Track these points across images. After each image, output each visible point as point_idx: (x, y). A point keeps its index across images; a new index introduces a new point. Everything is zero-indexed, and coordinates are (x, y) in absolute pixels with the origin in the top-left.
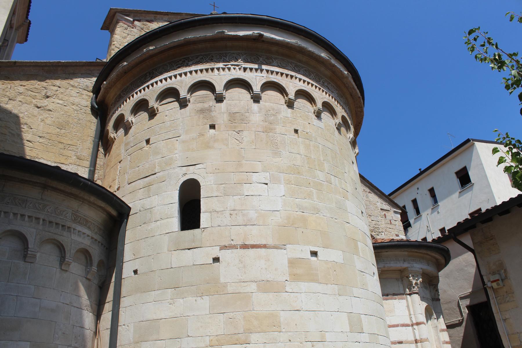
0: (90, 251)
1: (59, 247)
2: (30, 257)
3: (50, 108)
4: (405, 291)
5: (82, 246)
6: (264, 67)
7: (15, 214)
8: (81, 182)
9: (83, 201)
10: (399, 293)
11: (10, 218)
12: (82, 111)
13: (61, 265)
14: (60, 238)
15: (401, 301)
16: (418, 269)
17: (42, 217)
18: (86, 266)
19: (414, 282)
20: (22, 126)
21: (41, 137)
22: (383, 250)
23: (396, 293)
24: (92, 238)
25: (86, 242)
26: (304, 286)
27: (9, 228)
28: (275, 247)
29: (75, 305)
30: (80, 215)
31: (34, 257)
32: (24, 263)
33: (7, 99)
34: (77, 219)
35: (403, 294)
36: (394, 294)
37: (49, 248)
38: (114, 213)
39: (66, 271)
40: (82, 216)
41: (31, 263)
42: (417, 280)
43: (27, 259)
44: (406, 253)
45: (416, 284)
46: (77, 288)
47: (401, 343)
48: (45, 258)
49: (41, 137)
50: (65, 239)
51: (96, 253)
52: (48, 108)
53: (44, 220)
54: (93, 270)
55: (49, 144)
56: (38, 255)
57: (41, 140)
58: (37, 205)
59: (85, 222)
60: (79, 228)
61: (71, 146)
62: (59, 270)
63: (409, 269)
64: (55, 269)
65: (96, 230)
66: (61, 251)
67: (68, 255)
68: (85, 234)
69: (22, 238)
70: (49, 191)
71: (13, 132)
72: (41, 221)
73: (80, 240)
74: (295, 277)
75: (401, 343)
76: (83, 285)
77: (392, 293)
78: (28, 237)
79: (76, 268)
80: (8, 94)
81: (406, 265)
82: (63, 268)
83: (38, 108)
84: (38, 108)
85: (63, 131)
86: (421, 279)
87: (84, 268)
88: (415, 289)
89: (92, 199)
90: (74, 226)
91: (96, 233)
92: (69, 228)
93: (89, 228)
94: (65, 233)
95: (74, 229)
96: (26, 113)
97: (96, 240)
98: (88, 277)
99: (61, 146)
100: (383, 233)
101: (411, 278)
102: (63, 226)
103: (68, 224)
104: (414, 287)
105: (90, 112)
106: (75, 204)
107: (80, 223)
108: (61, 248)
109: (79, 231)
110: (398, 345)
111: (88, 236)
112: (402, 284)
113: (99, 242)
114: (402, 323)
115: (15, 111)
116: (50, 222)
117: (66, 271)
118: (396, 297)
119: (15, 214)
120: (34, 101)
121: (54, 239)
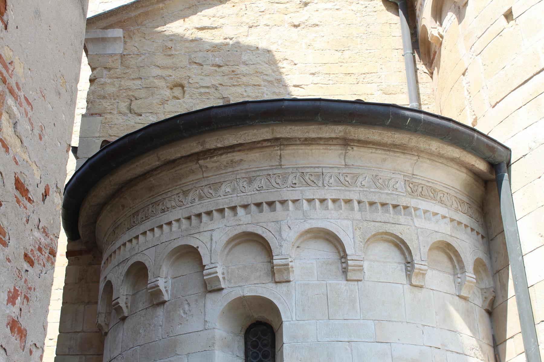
0: (455, 245)
1: (396, 245)
2: (354, 270)
3: (316, 22)
5: (439, 237)
7: (310, 201)
8: (406, 118)
9: (419, 152)
11: (305, 208)
12: (368, 10)
13: (409, 277)
14: (396, 230)
17: (355, 197)
18: (455, 275)
20: (280, 65)
21: (313, 74)
24: (452, 220)
25: (444, 230)
27: (307, 226)
30: (420, 182)
31: (360, 269)
32: (345, 282)
33: (246, 28)
34: (416, 189)
38: (481, 166)
39: (421, 287)
40: (424, 182)
41: (358, 281)
43: (350, 275)
46: (447, 317)
48: (379, 266)
49: (313, 74)
50: (405, 228)
51: (469, 247)
52: (311, 22)
53: (359, 202)
54: (468, 278)
55: (331, 82)
56: (366, 265)
57: (316, 79)
58: (342, 179)
59: (431, 193)
60: (423, 205)
61: (368, 76)
62: (407, 287)
64: (401, 286)
65: (455, 205)
66: (403, 254)
68: (437, 214)
69: (332, 239)
70: (355, 148)
71: (270, 79)
76: (457, 310)
78: (341, 236)
79: (437, 279)
80: (244, 19)
82: (414, 283)
83: (296, 26)
84: (296, 26)
85: (347, 54)
87: (451, 278)
89: (435, 145)
90: (413, 202)
91: (456, 210)
92: (406, 208)
93: (441, 202)
94: (402, 219)
95: (416, 209)
96: (280, 42)
97: (459, 223)
98: (462, 294)
99: (352, 79)
102: (395, 206)
103: (403, 201)
105: (383, 8)
106: (405, 163)
108: (401, 246)
109: (425, 212)
111: (444, 217)
113: (466, 226)
115: (263, 45)
116: (372, 204)
117: (421, 287)
119: (310, 201)
120: (286, 18)
121: (386, 233)
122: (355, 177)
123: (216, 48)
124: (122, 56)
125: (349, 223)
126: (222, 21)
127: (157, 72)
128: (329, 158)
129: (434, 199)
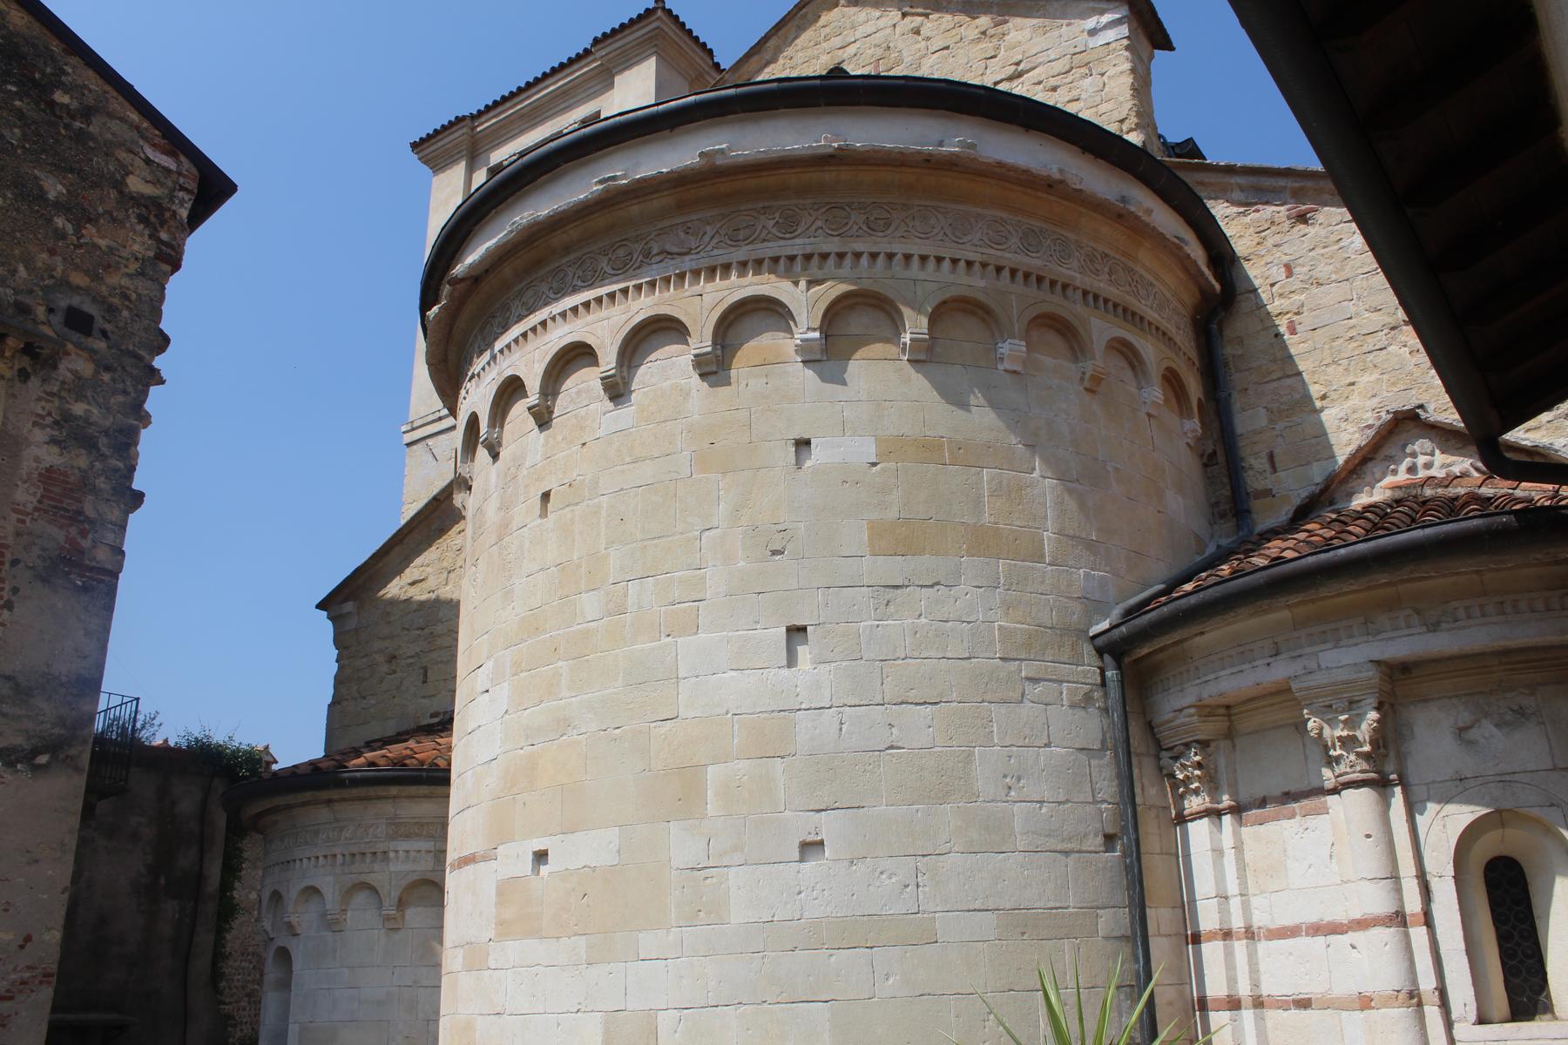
6: (498, 345)
10: (1304, 786)
14: (370, 879)
15: (1312, 821)
16: (1342, 675)
17: (337, 850)
26: (514, 949)
27: (303, 885)
28: (487, 858)
29: (425, 983)
36: (1289, 797)
37: (361, 898)
42: (1352, 724)
44: (1284, 615)
45: (1349, 742)
47: (1304, 1004)
48: (361, 914)
60: (403, 845)
63: (1294, 686)
67: (386, 903)
72: (339, 857)
73: (409, 867)
74: (505, 929)
75: (1304, 1004)
77: (1278, 793)
80: (445, 564)
86: (1373, 715)
90: (393, 845)
103: (381, 847)
106: (388, 808)
107: (407, 836)
110: (1295, 1014)
114: (1312, 918)
122: (341, 829)
123: (422, 604)
124: (356, 630)
125: (330, 878)
126: (429, 569)
127: (378, 645)
128: (323, 814)
129: (418, 835)
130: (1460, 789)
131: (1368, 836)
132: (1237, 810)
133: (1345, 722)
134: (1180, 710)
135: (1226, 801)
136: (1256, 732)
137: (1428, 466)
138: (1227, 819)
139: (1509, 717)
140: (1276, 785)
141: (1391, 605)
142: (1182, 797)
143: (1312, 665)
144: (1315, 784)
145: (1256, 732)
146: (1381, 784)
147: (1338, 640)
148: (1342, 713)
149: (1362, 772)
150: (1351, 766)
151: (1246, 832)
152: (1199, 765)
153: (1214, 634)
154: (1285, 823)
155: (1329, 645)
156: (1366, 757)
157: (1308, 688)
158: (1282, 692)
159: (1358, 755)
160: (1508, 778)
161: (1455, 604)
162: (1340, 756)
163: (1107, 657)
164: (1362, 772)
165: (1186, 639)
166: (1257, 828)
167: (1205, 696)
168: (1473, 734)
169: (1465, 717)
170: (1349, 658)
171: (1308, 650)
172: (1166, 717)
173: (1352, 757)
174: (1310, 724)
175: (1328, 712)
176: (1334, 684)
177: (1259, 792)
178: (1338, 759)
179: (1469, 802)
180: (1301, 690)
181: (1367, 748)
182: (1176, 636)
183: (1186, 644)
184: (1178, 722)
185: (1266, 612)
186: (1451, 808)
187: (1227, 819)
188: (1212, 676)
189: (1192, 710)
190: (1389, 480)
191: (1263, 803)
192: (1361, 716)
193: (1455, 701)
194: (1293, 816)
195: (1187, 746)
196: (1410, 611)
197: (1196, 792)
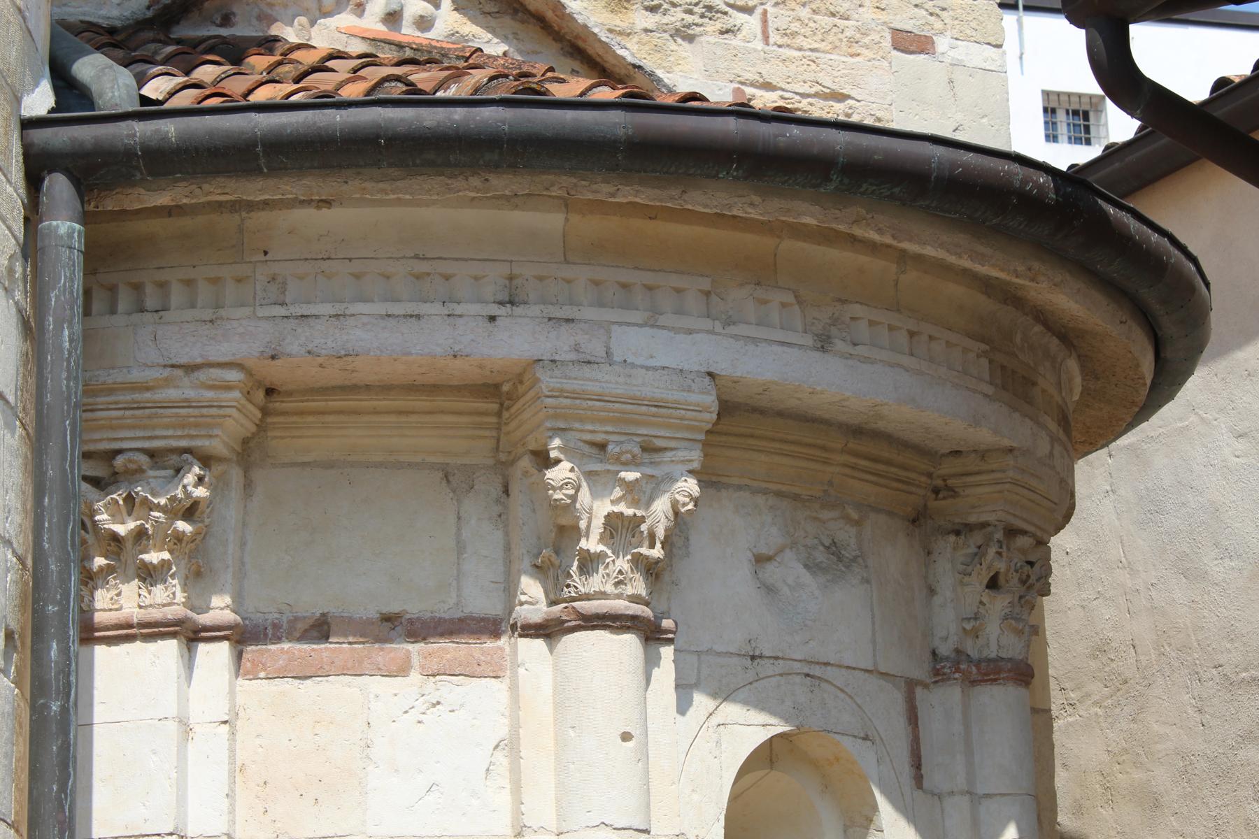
4: (510, 590)
10: (445, 608)
15: (451, 690)
16: (651, 387)
19: (597, 509)
22: (289, 187)
23: (414, 607)
35: (491, 627)
36: (395, 626)
42: (638, 494)
44: (550, 221)
45: (618, 529)
63: (548, 380)
81: (514, 341)
88: (596, 583)
100: (751, 23)
101: (560, 473)
104: (589, 563)
112: (502, 518)
118: (415, 649)
130: (751, 676)
131: (626, 737)
132: (242, 637)
133: (630, 487)
134: (190, 368)
135: (220, 609)
136: (329, 465)
137: (424, 23)
138: (215, 655)
139: (820, 556)
140: (366, 593)
141: (761, 273)
142: (90, 579)
143: (595, 348)
144: (481, 603)
145: (329, 465)
146: (652, 634)
147: (655, 311)
148: (632, 464)
149: (635, 599)
150: (613, 583)
151: (255, 691)
152: (190, 511)
153: (364, 213)
154: (377, 685)
155: (637, 317)
156: (651, 570)
157: (576, 395)
158: (498, 394)
159: (638, 561)
160: (817, 671)
161: (857, 310)
162: (600, 557)
163: (58, 186)
164: (635, 599)
165: (251, 206)
166: (288, 685)
167: (293, 346)
168: (771, 572)
169: (772, 537)
170: (669, 355)
171: (590, 313)
172: (136, 375)
173: (623, 563)
174: (556, 475)
175: (596, 454)
176: (635, 401)
177: (311, 603)
178: (589, 563)
179: (760, 704)
180: (561, 393)
181: (657, 552)
182: (253, 189)
183: (262, 217)
184: (172, 394)
185: (512, 200)
186: (732, 711)
187: (215, 655)
188: (325, 309)
189: (234, 376)
190: (345, 20)
191: (320, 630)
192: (656, 485)
193: (760, 499)
194: (402, 670)
195: (168, 461)
196: (790, 298)
197: (150, 575)
